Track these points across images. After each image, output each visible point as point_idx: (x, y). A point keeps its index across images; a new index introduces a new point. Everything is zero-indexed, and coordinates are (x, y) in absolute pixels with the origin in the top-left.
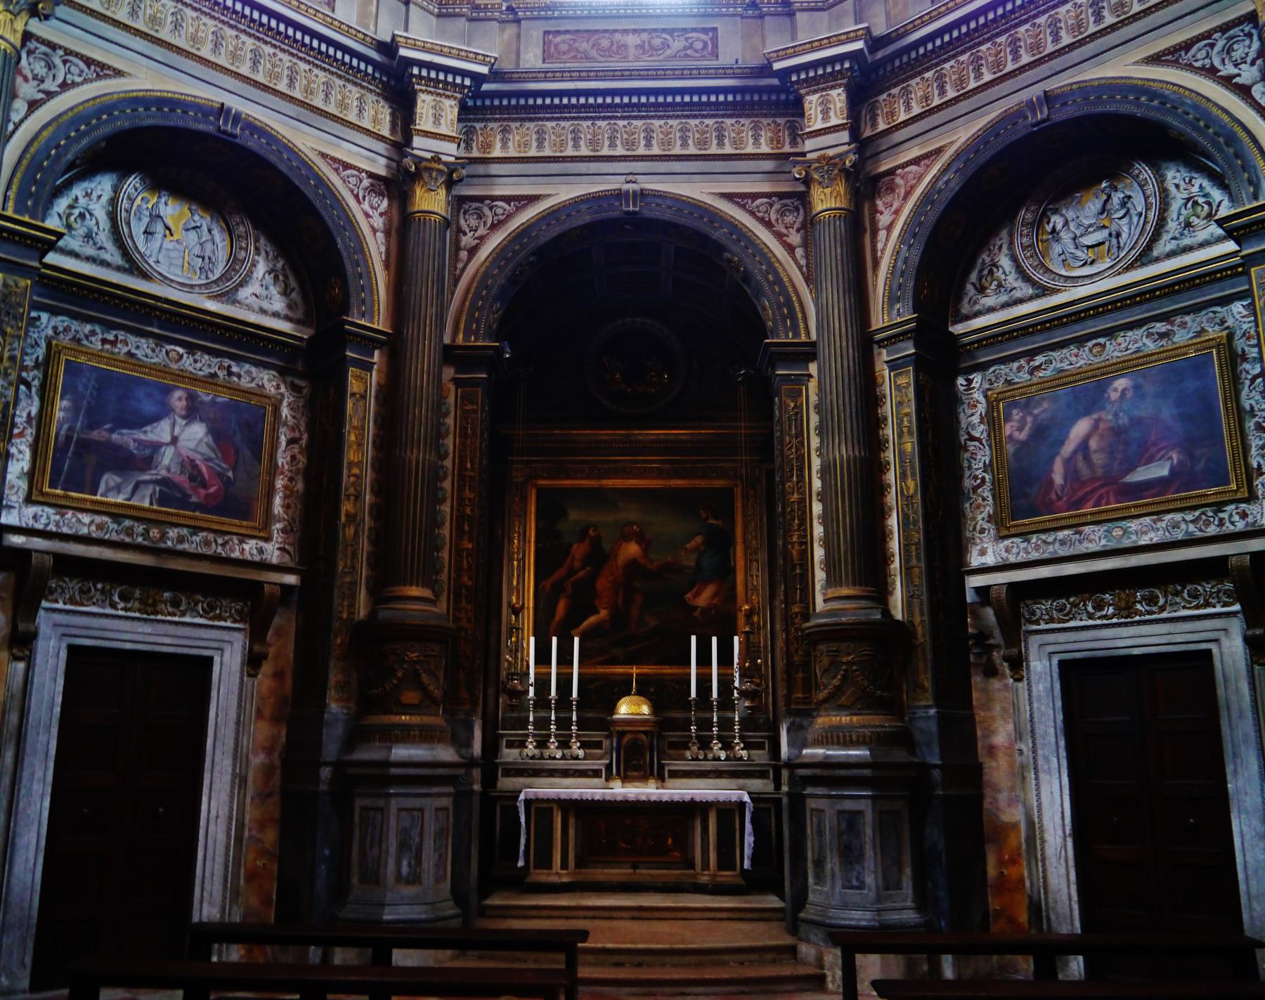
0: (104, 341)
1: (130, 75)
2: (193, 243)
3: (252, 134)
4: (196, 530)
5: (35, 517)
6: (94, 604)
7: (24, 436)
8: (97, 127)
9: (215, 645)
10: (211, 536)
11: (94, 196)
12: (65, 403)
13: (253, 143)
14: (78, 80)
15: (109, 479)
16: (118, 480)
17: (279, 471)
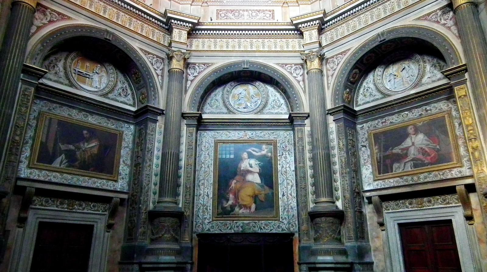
0: (382, 123)
2: (405, 74)
4: (430, 172)
5: (377, 185)
6: (401, 208)
7: (368, 162)
9: (450, 214)
10: (437, 173)
11: (369, 83)
12: (377, 147)
13: (391, 37)
15: (395, 165)
16: (398, 164)
17: (458, 138)
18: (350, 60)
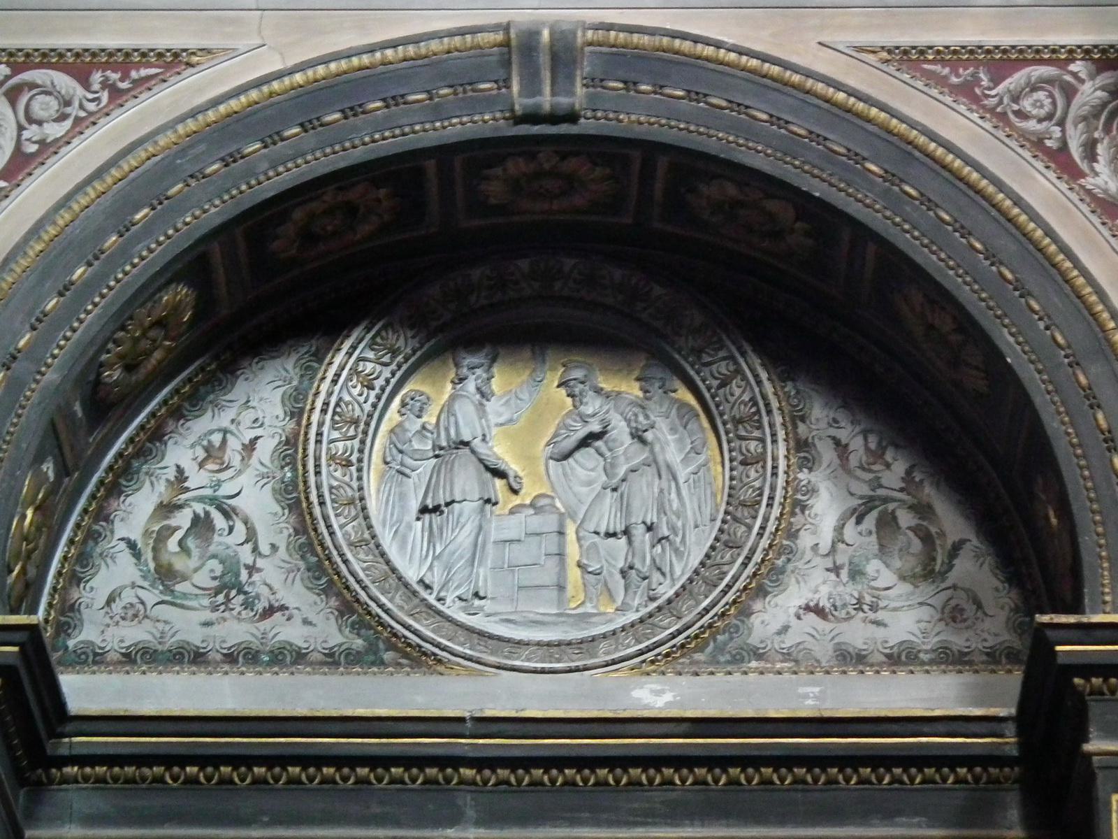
1: (208, 51)
2: (587, 494)
3: (630, 84)
8: (123, 253)
11: (233, 452)
14: (54, 131)
18: (166, 169)
